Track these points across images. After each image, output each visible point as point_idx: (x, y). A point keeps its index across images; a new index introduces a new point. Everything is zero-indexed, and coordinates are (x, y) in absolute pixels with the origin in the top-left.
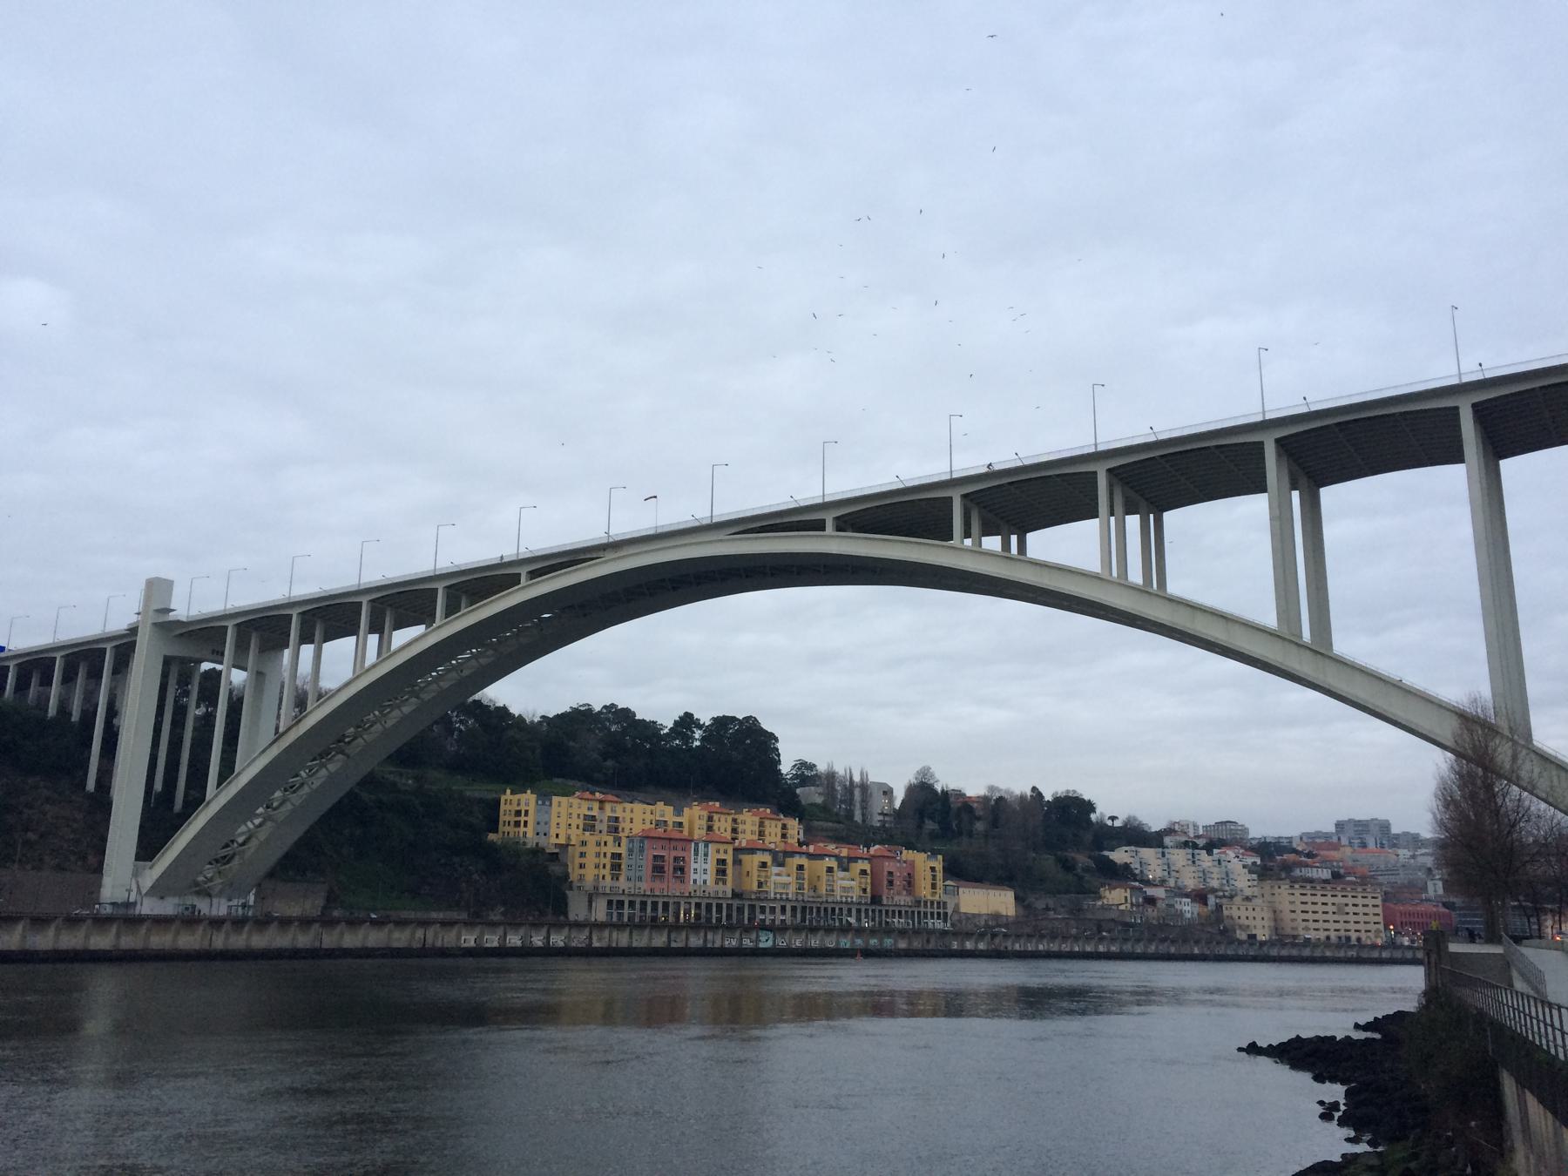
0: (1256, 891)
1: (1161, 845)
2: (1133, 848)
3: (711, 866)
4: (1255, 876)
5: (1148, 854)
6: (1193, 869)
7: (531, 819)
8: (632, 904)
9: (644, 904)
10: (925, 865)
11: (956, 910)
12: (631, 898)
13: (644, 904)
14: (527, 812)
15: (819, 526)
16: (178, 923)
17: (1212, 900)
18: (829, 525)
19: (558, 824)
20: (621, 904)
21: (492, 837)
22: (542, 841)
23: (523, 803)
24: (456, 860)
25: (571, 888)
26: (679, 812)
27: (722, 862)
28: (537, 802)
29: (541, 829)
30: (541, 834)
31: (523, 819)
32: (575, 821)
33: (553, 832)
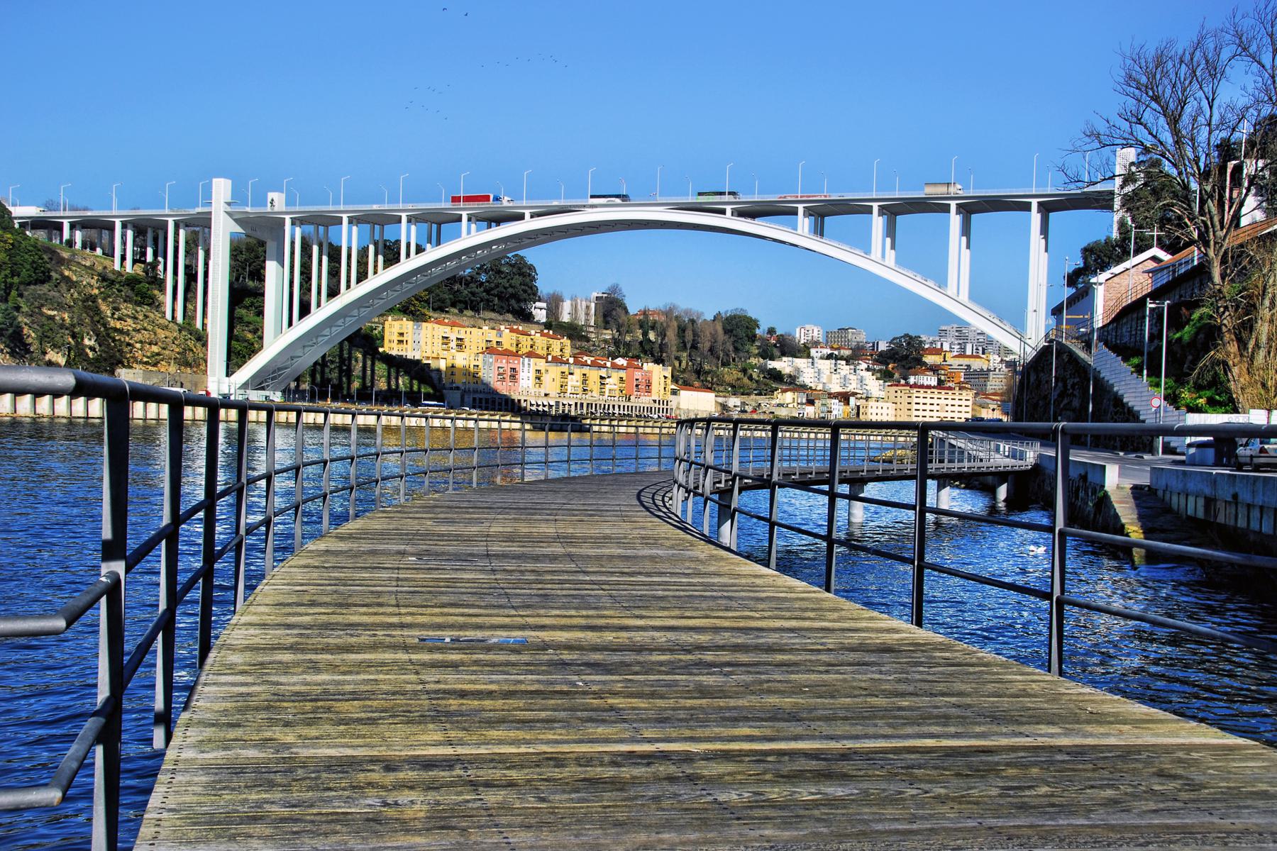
0: (882, 394)
1: (809, 356)
2: (790, 359)
3: (532, 375)
4: (881, 382)
5: (801, 363)
6: (838, 376)
10: (658, 373)
11: (678, 408)
15: (723, 212)
17: (852, 400)
18: (729, 212)
23: (404, 327)
26: (500, 334)
27: (539, 371)
31: (404, 339)
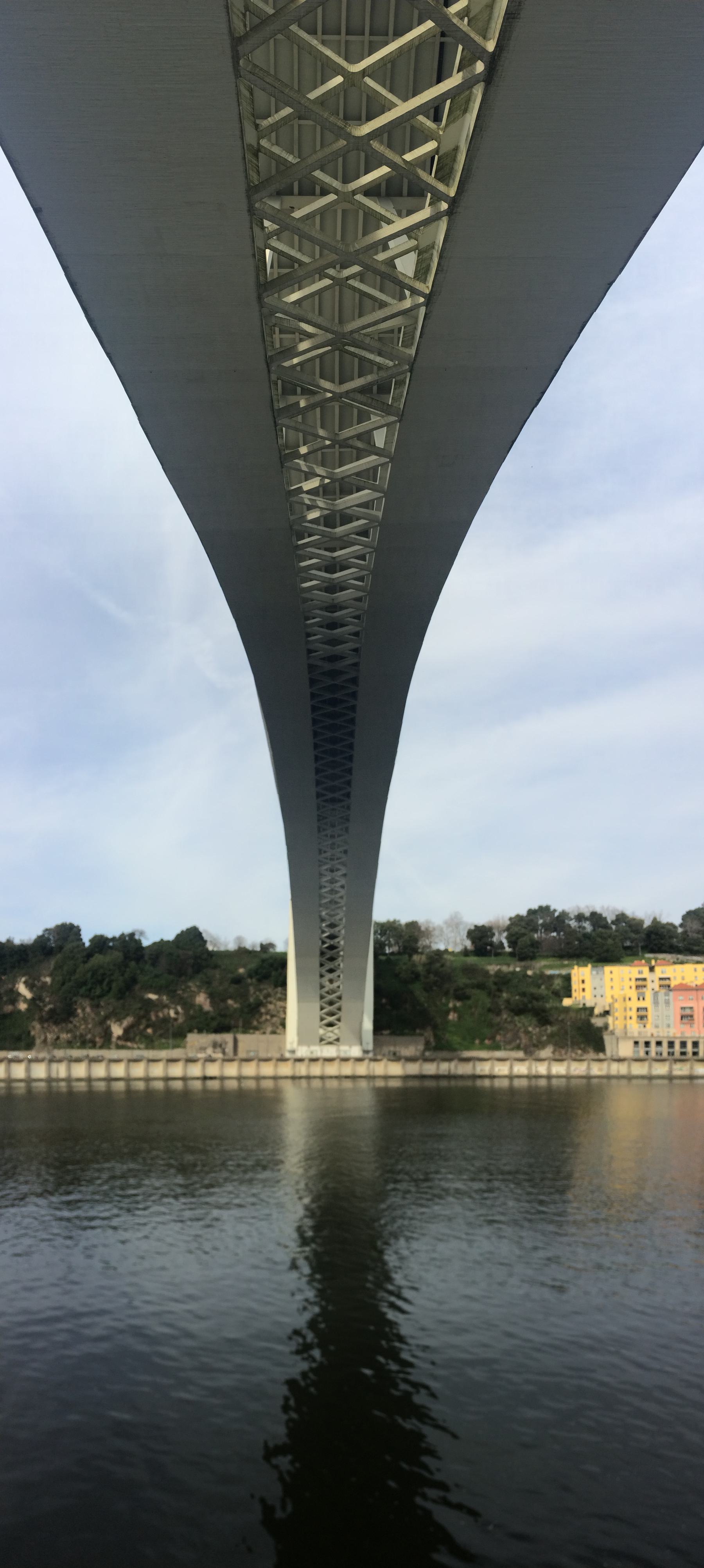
7: (587, 985)
8: (659, 1043)
9: (671, 1044)
12: (659, 1040)
13: (671, 1044)
14: (583, 982)
16: (306, 1062)
19: (612, 987)
20: (647, 1044)
21: (567, 1002)
22: (599, 1000)
24: (516, 1018)
25: (612, 1033)
28: (591, 973)
29: (599, 992)
30: (599, 997)
32: (627, 984)
33: (608, 993)
